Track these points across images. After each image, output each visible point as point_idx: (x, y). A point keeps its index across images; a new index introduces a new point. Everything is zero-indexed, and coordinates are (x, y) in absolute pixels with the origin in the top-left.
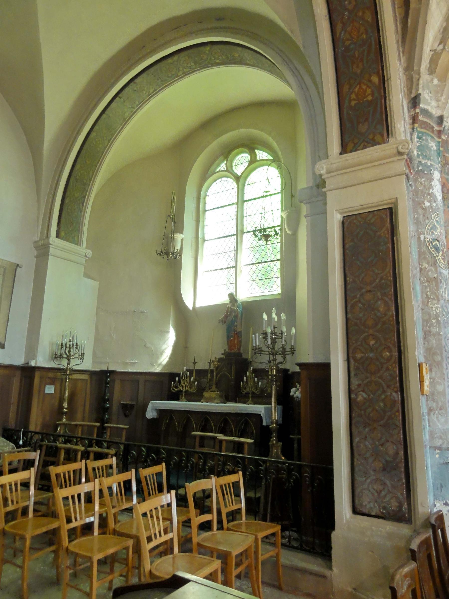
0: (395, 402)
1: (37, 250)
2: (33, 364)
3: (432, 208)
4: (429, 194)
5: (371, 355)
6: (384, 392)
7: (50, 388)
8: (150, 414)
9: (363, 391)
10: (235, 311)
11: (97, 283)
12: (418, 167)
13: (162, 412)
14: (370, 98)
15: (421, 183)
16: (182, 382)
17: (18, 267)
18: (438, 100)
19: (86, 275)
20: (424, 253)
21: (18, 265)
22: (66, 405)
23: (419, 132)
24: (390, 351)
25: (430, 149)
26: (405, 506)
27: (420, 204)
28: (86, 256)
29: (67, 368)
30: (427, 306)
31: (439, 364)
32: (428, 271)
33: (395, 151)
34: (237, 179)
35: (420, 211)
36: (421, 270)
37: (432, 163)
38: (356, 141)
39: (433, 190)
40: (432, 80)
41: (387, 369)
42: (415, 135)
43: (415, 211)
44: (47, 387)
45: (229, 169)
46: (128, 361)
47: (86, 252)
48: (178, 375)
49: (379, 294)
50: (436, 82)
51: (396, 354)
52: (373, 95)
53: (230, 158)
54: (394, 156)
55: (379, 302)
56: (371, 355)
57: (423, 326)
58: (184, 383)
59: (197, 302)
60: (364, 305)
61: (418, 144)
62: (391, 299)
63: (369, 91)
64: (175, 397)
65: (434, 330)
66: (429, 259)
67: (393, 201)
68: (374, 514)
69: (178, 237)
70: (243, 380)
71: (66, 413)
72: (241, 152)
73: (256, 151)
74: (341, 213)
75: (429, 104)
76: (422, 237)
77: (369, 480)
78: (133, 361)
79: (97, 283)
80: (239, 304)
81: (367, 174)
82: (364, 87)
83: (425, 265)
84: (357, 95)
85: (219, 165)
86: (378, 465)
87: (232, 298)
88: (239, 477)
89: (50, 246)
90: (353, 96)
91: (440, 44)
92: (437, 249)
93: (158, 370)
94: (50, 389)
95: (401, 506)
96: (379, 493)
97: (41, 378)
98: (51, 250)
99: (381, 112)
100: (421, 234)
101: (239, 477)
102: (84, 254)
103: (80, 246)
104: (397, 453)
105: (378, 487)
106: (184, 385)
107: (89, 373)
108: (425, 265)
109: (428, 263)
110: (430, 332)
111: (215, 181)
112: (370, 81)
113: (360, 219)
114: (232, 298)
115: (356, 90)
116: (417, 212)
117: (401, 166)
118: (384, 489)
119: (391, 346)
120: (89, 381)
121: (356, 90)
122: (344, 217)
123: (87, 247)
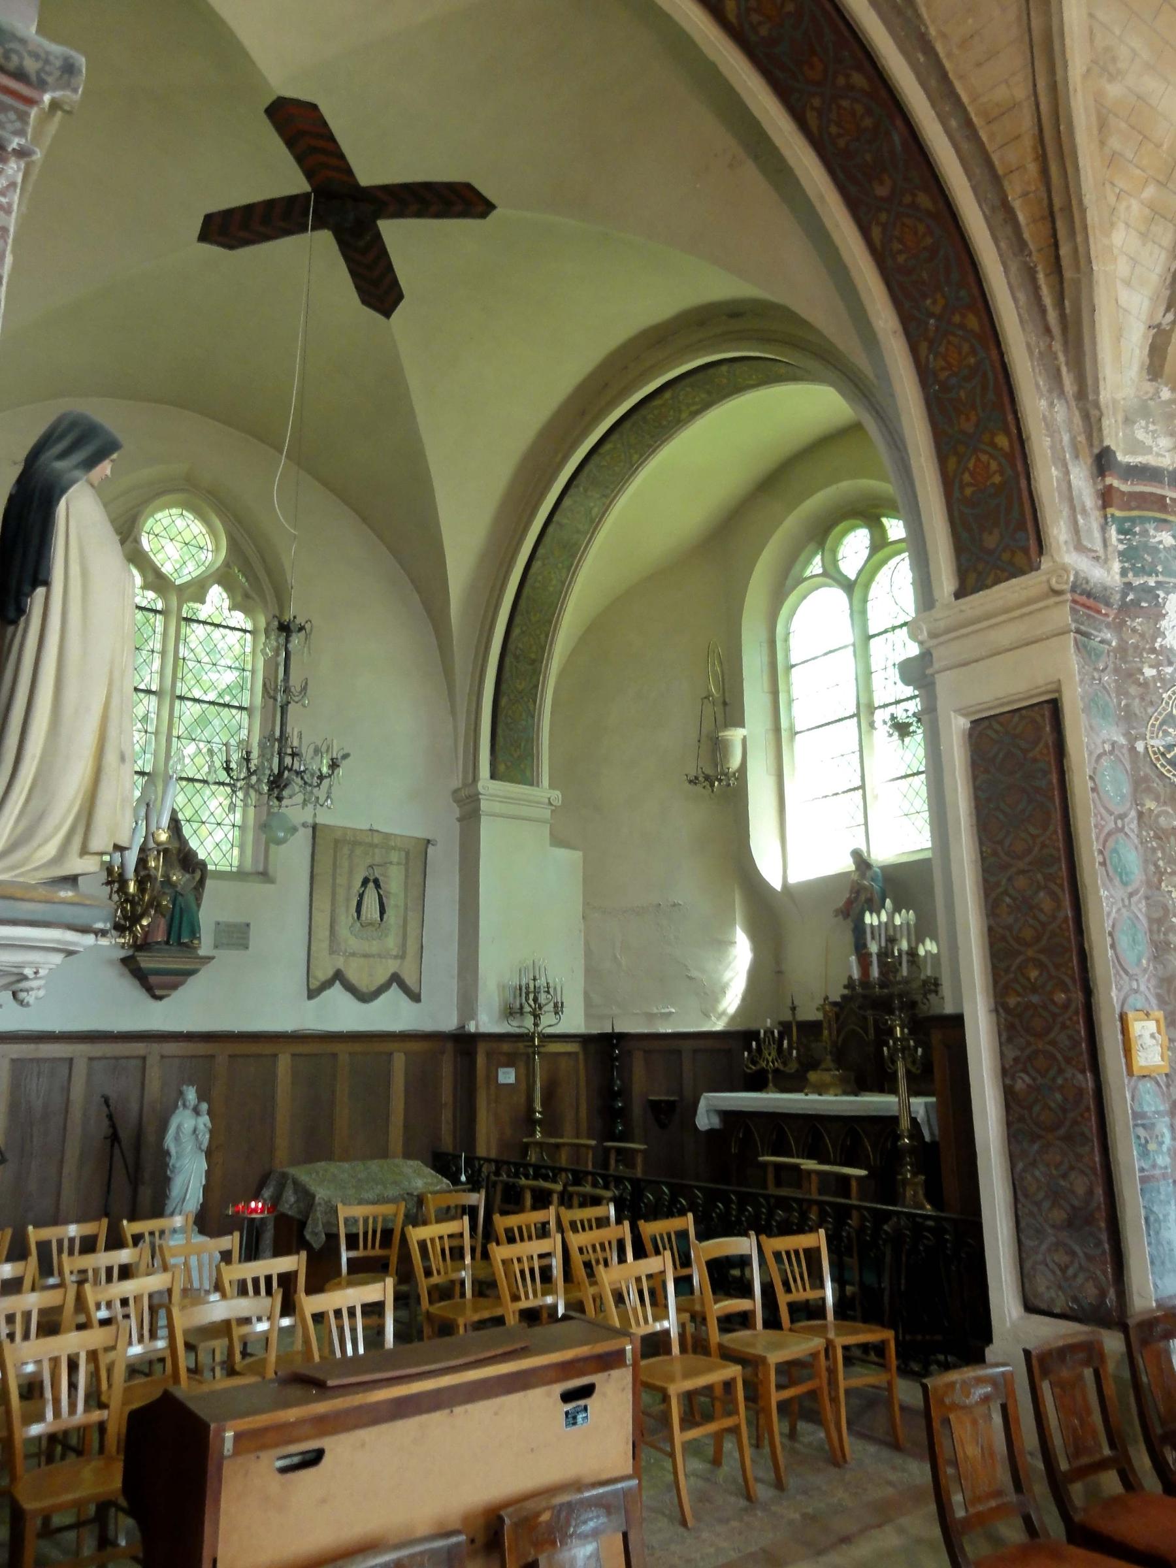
0: (1080, 1092)
1: (460, 807)
2: (472, 1028)
3: (1163, 680)
4: (1153, 650)
5: (1035, 999)
6: (1061, 1071)
7: (508, 1073)
8: (704, 1120)
9: (1025, 1071)
10: (865, 888)
11: (577, 855)
12: (1125, 595)
13: (730, 1117)
14: (997, 479)
15: (1134, 630)
16: (766, 1053)
17: (430, 846)
19: (558, 841)
20: (1146, 779)
21: (429, 841)
22: (538, 1107)
23: (1120, 522)
24: (1066, 990)
25: (1155, 550)
26: (1112, 1293)
27: (1132, 675)
28: (550, 804)
29: (534, 1033)
30: (1159, 888)
32: (1158, 816)
33: (1045, 588)
34: (848, 587)
35: (1133, 690)
36: (1140, 815)
37: (1160, 578)
38: (980, 567)
39: (1164, 637)
40: (1157, 392)
41: (1064, 1027)
42: (1113, 532)
43: (1121, 692)
44: (501, 1071)
45: (831, 571)
46: (655, 1011)
47: (549, 796)
49: (1039, 876)
51: (1079, 996)
52: (1001, 472)
53: (829, 544)
54: (1045, 597)
55: (1042, 894)
56: (1035, 999)
57: (1151, 931)
58: (770, 1054)
59: (789, 872)
60: (1014, 899)
61: (1121, 547)
62: (1061, 886)
63: (994, 466)
64: (756, 1083)
66: (1160, 789)
67: (1054, 686)
68: (1057, 1310)
69: (736, 735)
70: (887, 1045)
71: (539, 1122)
72: (853, 528)
73: (884, 520)
74: (965, 715)
75: (1149, 450)
76: (1140, 746)
77: (1044, 1247)
78: (667, 1010)
79: (577, 855)
80: (876, 873)
81: (1004, 635)
82: (984, 458)
83: (1151, 804)
84: (972, 475)
85: (808, 562)
86: (1059, 1215)
87: (861, 861)
88: (819, 1239)
89: (481, 797)
90: (967, 477)
91: (1168, 310)
93: (719, 1026)
94: (507, 1076)
95: (1103, 1294)
96: (1063, 1270)
97: (489, 1055)
98: (484, 805)
99: (1021, 504)
100: (1136, 739)
101: (819, 1239)
102: (547, 801)
103: (538, 786)
104: (1090, 1193)
105: (1061, 1258)
106: (770, 1059)
107: (579, 1039)
108: (1151, 804)
109: (1157, 799)
110: (1168, 943)
111: (805, 597)
112: (993, 445)
113: (996, 726)
114: (861, 861)
115: (971, 465)
116: (1126, 694)
117: (1063, 616)
118: (1072, 1262)
119: (1068, 980)
120: (581, 1056)
121: (971, 465)
122: (972, 722)
123: (552, 786)
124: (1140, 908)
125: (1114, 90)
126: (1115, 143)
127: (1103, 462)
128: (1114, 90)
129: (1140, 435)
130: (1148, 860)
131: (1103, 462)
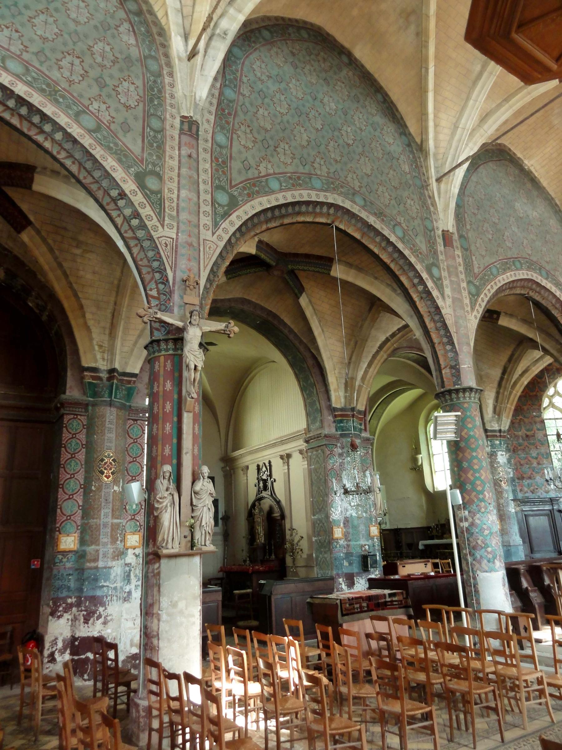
8: (421, 547)
13: (426, 546)
31: (504, 520)
48: (430, 527)
64: (432, 538)
69: (419, 456)
92: (501, 481)
127: (486, 431)
128: (483, 373)
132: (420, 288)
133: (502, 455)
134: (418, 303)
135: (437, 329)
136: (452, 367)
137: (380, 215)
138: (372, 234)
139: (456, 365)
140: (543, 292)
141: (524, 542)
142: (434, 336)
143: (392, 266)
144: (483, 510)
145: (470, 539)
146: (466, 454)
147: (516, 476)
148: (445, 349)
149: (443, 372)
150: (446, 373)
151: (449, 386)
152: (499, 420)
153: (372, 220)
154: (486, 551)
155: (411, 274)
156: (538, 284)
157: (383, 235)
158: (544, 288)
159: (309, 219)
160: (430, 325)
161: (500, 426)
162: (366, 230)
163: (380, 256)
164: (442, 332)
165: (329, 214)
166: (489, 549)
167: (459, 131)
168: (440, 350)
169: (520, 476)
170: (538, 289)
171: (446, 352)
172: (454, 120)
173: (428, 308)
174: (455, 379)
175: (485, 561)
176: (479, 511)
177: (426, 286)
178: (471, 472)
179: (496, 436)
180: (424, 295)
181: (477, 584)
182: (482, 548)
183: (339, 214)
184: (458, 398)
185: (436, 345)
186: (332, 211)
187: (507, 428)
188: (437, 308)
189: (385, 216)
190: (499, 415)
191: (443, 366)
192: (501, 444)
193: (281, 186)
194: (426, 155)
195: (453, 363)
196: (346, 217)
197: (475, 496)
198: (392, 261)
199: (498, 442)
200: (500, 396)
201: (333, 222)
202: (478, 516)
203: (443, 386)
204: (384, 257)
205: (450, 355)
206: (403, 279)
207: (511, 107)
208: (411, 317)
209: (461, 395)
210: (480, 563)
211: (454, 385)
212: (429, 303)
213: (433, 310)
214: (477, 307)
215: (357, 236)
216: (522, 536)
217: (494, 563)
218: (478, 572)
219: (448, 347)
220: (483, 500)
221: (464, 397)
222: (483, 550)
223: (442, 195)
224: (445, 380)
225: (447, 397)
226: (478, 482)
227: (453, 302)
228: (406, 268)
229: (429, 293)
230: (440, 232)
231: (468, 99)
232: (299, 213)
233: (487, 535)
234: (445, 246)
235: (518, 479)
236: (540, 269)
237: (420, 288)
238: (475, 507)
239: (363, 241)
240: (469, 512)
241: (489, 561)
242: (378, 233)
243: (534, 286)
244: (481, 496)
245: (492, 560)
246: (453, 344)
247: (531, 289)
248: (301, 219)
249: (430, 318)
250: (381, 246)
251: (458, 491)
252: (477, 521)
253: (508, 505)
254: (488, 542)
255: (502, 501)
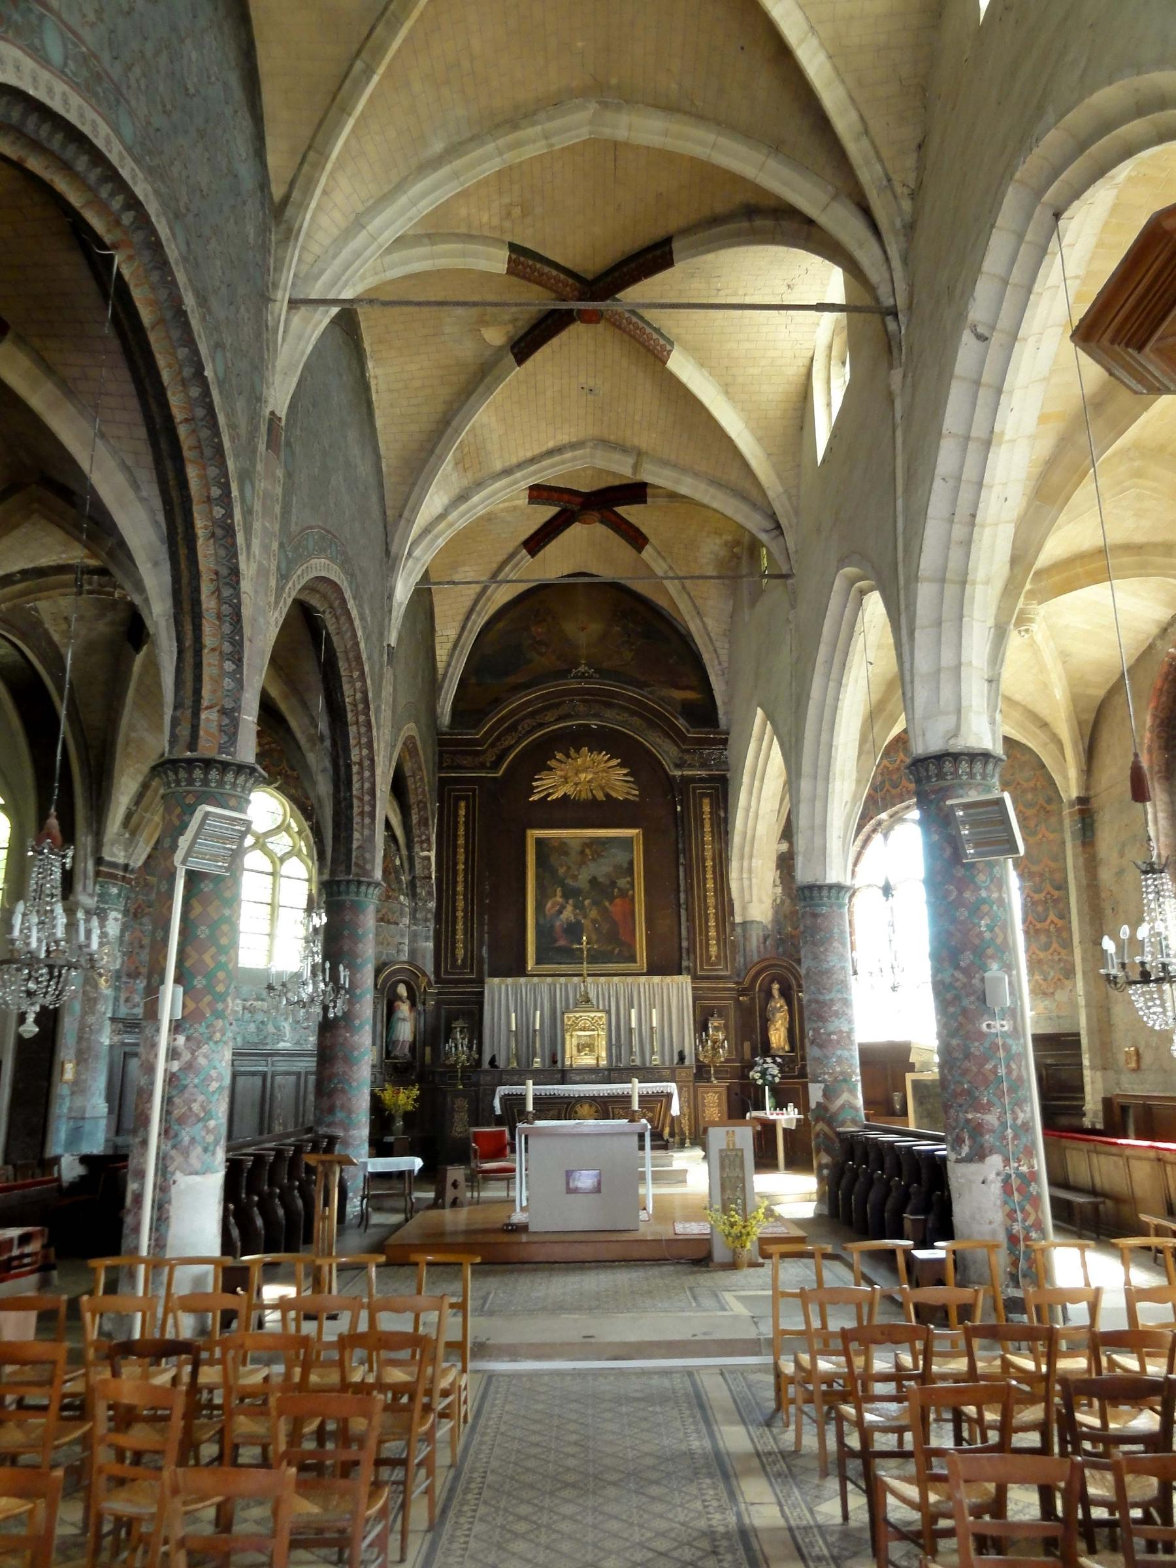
18: (126, 850)
25: (110, 895)
31: (86, 1060)
42: (98, 887)
50: (127, 835)
65: (86, 1036)
75: (116, 856)
124: (76, 1025)
125: (133, 735)
126: (130, 750)
127: (99, 861)
128: (133, 735)
129: (115, 850)
130: (83, 1008)
131: (99, 861)
132: (218, 512)
133: (116, 919)
134: (200, 542)
135: (219, 616)
136: (223, 712)
137: (202, 301)
138: (176, 334)
139: (233, 710)
140: (343, 619)
141: (110, 1112)
142: (207, 629)
143: (182, 431)
144: (218, 1035)
145: (177, 1100)
146: (211, 909)
147: (125, 968)
148: (221, 667)
149: (203, 716)
150: (207, 720)
151: (207, 747)
152: (130, 843)
153: (189, 301)
154: (205, 1127)
155: (212, 471)
156: (344, 602)
157: (196, 352)
158: (348, 613)
159: (75, 199)
160: (208, 603)
161: (129, 857)
162: (169, 315)
163: (169, 393)
164: (227, 628)
165: (118, 222)
166: (212, 1123)
167: (362, 236)
168: (210, 665)
169: (133, 968)
170: (339, 612)
171: (223, 674)
172: (360, 208)
173: (217, 563)
174: (225, 738)
175: (199, 1150)
176: (210, 1038)
177: (229, 514)
178: (213, 950)
179: (114, 876)
180: (219, 532)
181: (169, 1202)
182: (199, 1120)
183: (138, 237)
184: (221, 783)
185: (206, 651)
186: (127, 218)
187: (140, 863)
188: (235, 572)
189: (209, 312)
190: (133, 833)
191: (205, 703)
192: (119, 895)
193: (66, 65)
194: (289, 235)
195: (229, 704)
196: (147, 256)
197: (209, 1004)
198: (186, 420)
199: (115, 891)
200: (149, 793)
201: (115, 247)
202: (205, 1049)
203: (193, 745)
204: (175, 401)
205: (228, 683)
206: (192, 472)
207: (433, 256)
208: (156, 564)
209: (230, 777)
210: (186, 1153)
211: (220, 752)
212: (222, 552)
213: (224, 572)
214: (281, 604)
215: (146, 316)
216: (109, 1099)
217: (214, 1154)
218: (178, 1176)
219: (229, 666)
220: (219, 1015)
221: (234, 785)
222: (200, 1125)
223: (289, 338)
224: (202, 733)
225: (198, 773)
226: (221, 975)
227: (259, 571)
228: (208, 452)
229: (230, 531)
230: (267, 412)
231: (400, 187)
232: (66, 167)
233: (214, 1093)
234: (268, 447)
235: (129, 975)
236: (351, 576)
237: (218, 512)
238: (202, 1029)
239: (152, 337)
240: (188, 1039)
241: (206, 1150)
242: (189, 340)
243: (336, 603)
244: (220, 1006)
245: (211, 1148)
246: (239, 662)
247: (331, 607)
248: (61, 184)
249: (212, 587)
250: (180, 372)
251: (181, 989)
252: (202, 1061)
253: (100, 1031)
254: (212, 1107)
255: (91, 1019)
